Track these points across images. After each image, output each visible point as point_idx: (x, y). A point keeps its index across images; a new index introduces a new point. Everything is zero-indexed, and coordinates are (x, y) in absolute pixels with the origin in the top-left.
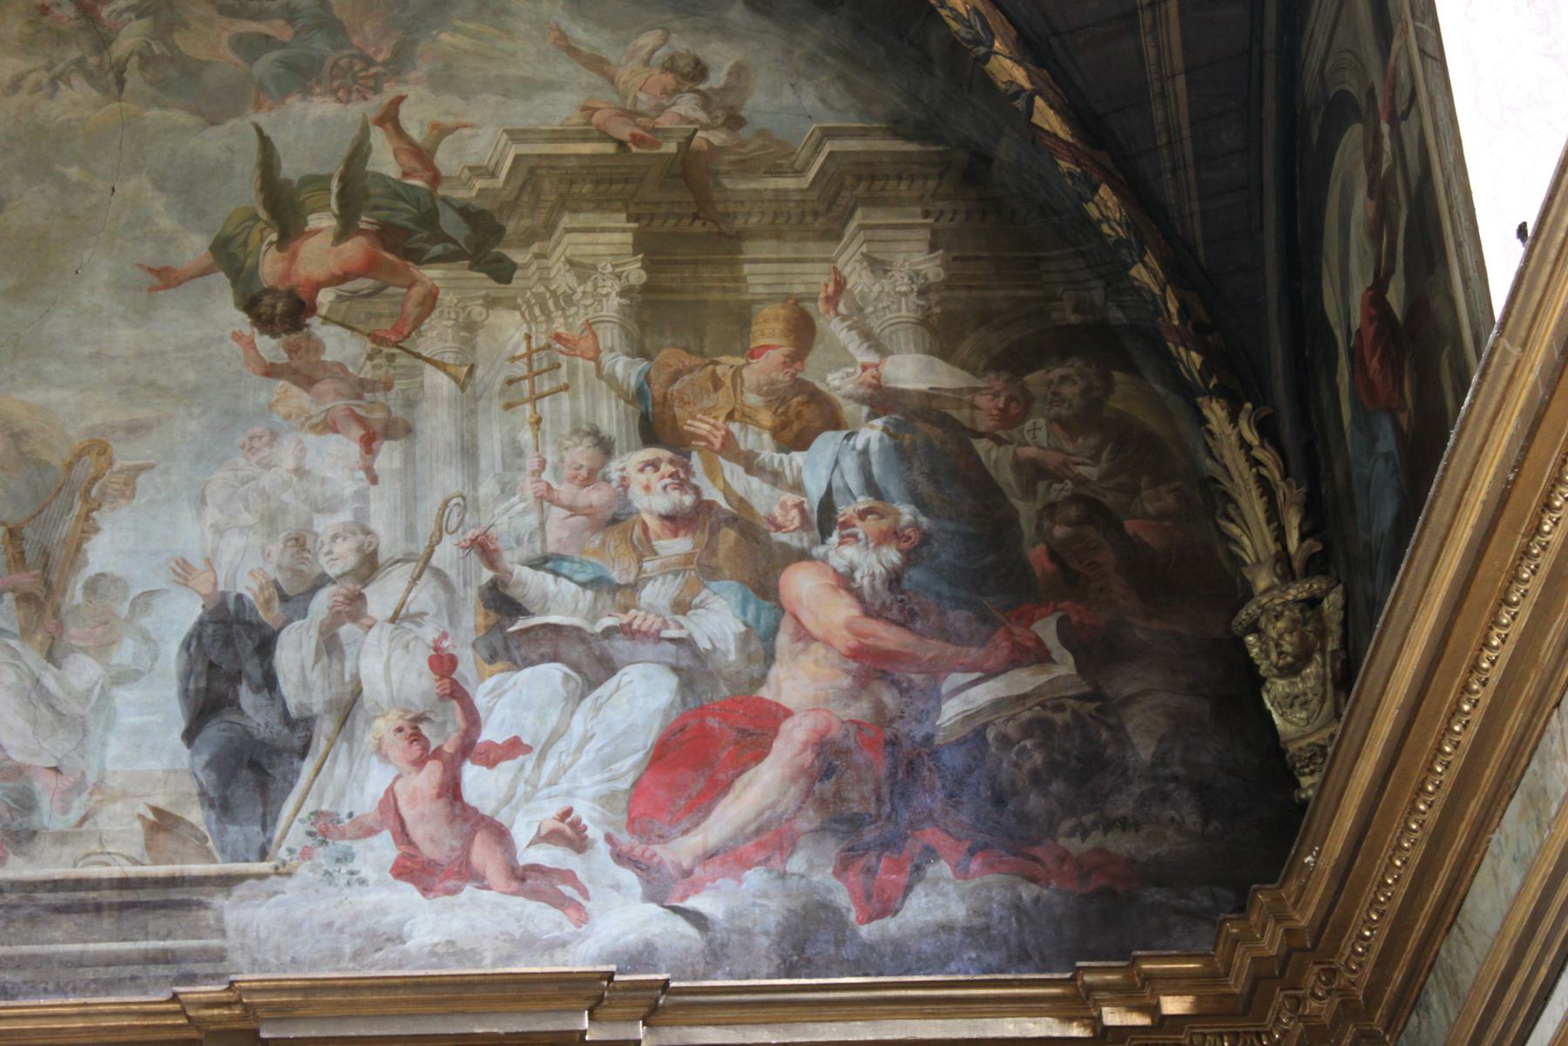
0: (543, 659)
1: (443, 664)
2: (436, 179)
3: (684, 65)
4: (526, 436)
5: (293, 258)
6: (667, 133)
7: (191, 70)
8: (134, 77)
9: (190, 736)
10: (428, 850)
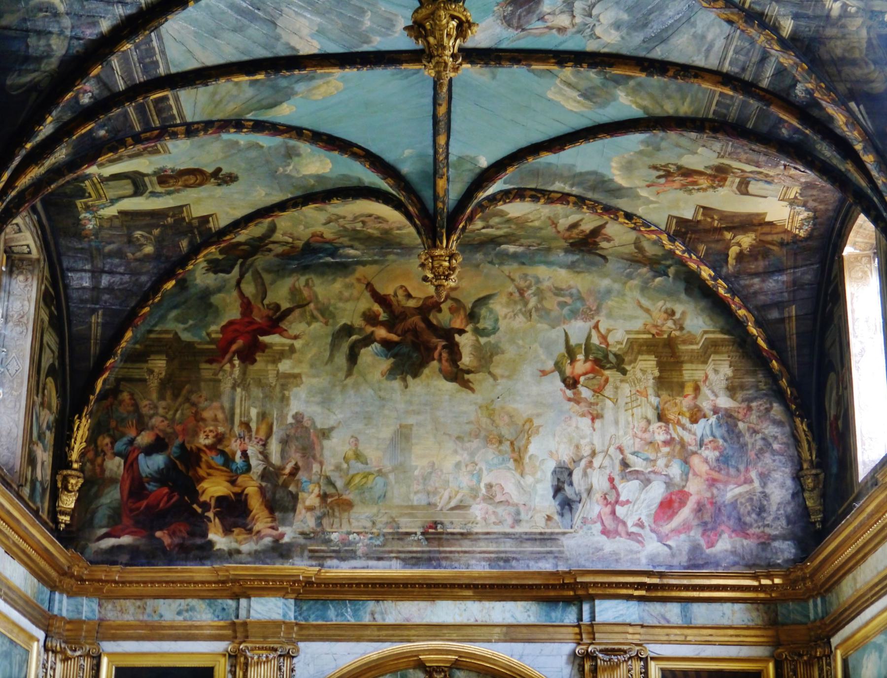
0: (634, 479)
1: (611, 480)
2: (608, 345)
3: (669, 311)
4: (630, 419)
5: (574, 368)
6: (664, 332)
7: (548, 312)
8: (534, 315)
9: (554, 497)
10: (608, 527)
